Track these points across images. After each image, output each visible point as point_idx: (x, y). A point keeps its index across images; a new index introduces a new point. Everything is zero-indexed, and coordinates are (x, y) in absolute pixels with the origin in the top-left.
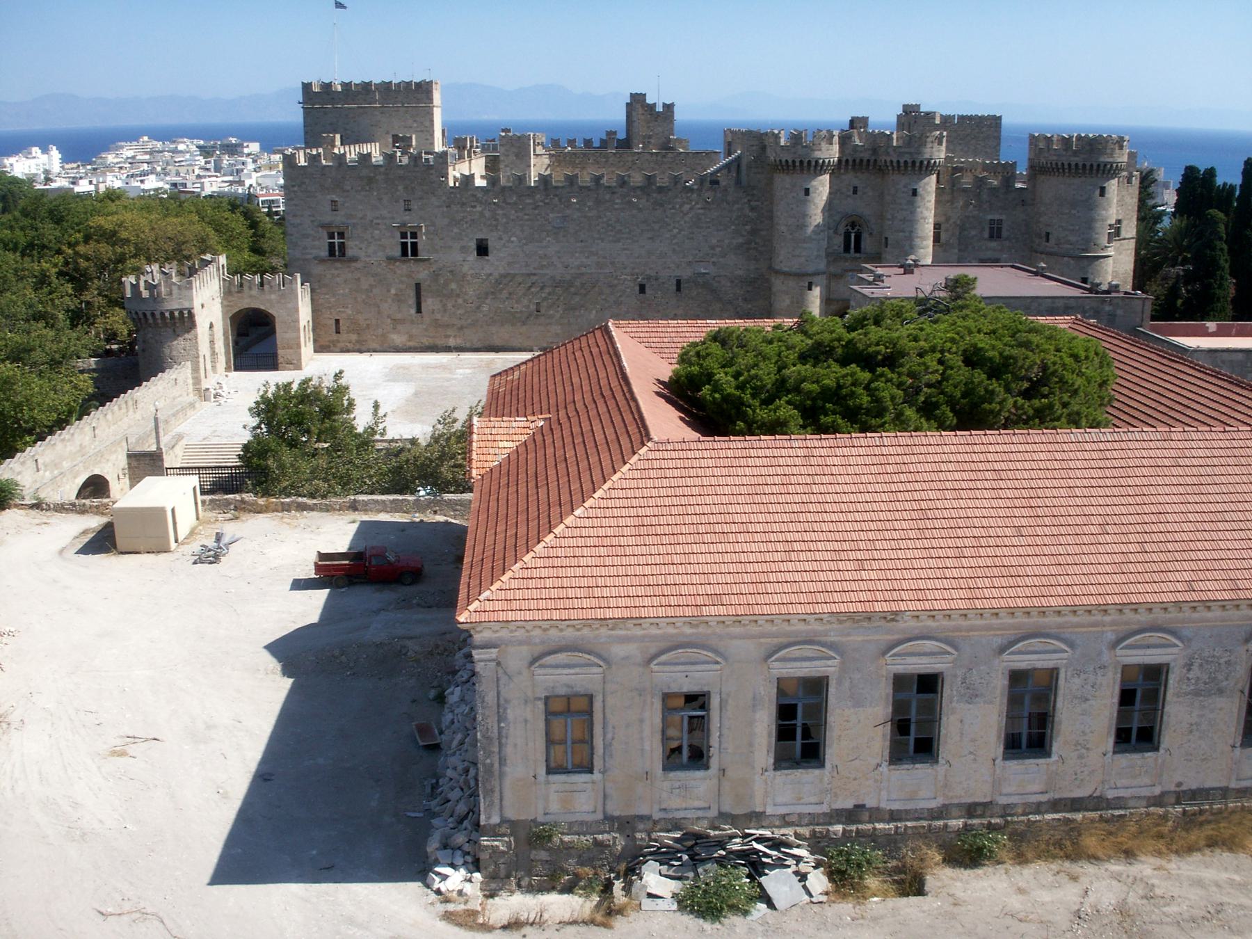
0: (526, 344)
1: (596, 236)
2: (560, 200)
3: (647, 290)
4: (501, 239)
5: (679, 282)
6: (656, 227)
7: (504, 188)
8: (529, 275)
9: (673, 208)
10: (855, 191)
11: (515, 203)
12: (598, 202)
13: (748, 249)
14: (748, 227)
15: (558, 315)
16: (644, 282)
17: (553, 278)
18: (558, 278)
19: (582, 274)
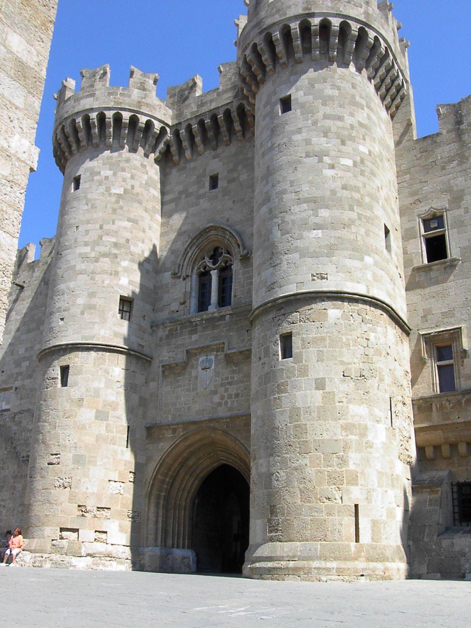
10: (214, 182)
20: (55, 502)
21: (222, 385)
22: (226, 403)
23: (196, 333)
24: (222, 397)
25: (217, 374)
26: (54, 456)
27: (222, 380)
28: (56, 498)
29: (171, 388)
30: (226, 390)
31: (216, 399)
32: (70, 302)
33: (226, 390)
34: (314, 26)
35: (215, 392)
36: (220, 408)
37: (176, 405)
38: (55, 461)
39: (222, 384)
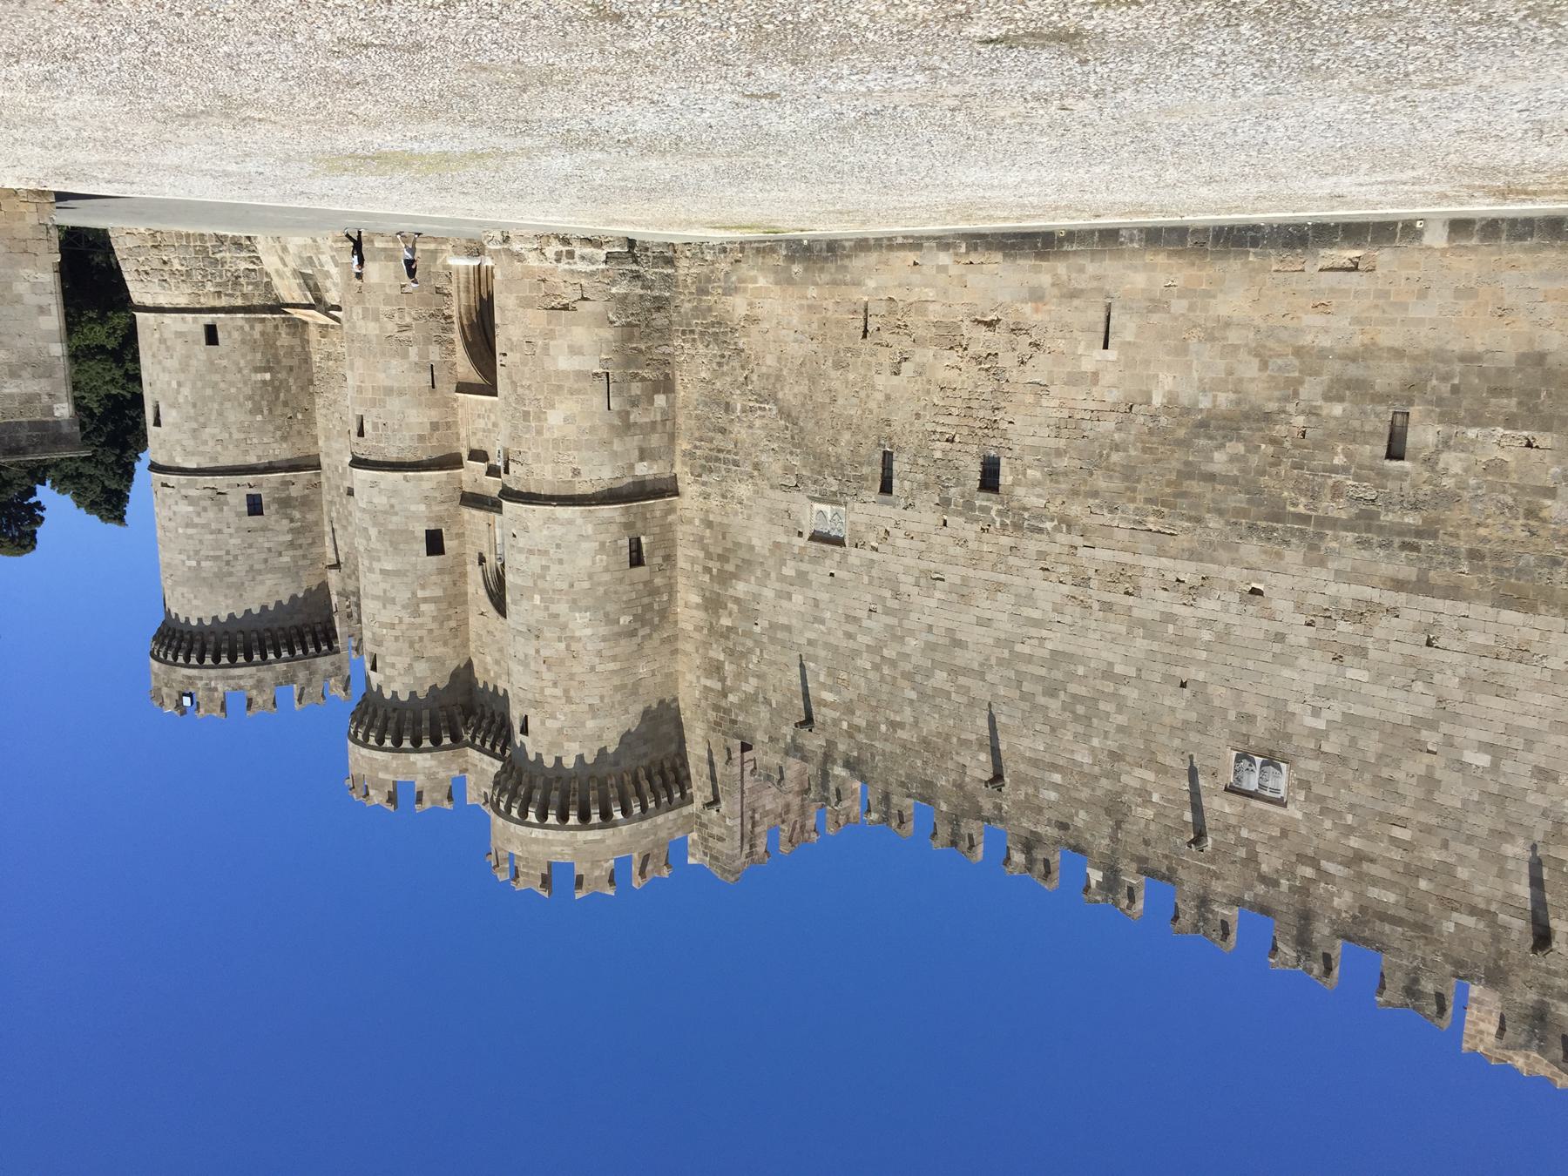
0: (1472, 262)
1: (1131, 694)
2: (1252, 859)
3: (974, 471)
4: (1545, 775)
5: (886, 488)
6: (940, 677)
7: (1496, 978)
8: (1422, 587)
9: (894, 725)
11: (1449, 905)
12: (1115, 810)
13: (723, 558)
14: (726, 622)
15: (1311, 390)
16: (982, 500)
17: (1316, 556)
18: (1293, 556)
19: (1193, 555)
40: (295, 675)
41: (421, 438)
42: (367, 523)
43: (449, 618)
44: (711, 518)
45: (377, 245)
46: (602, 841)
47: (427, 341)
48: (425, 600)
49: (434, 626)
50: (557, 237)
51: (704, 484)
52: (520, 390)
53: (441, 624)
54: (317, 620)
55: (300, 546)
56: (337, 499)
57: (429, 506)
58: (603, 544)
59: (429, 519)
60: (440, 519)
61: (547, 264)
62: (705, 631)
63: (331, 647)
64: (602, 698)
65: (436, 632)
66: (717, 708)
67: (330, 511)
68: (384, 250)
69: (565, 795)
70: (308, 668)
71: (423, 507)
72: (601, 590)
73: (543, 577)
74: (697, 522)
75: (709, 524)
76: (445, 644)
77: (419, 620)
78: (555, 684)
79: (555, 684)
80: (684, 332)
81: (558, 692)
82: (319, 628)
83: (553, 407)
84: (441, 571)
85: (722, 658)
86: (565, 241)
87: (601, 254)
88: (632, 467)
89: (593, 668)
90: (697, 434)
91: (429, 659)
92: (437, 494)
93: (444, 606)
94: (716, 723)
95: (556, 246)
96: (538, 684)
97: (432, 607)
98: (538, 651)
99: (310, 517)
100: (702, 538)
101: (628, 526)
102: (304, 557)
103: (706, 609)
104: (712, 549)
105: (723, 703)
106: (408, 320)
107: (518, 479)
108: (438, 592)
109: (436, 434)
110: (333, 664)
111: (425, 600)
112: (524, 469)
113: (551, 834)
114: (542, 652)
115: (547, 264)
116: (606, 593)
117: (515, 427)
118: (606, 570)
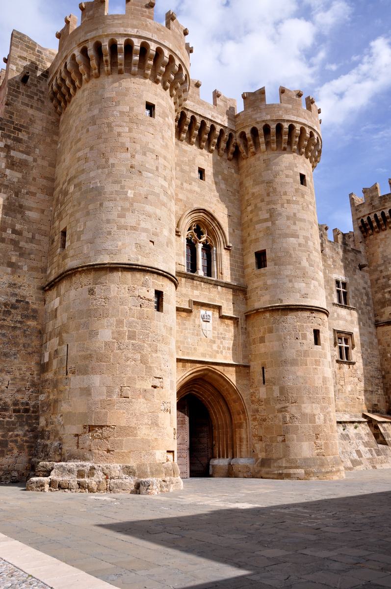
20: (162, 426)
21: (218, 338)
22: (222, 352)
23: (197, 290)
24: (219, 347)
25: (214, 328)
26: (157, 380)
27: (218, 334)
28: (163, 422)
29: (180, 328)
30: (222, 342)
31: (215, 347)
32: (158, 229)
33: (222, 342)
34: (120, 44)
35: (214, 342)
36: (218, 355)
37: (184, 344)
38: (158, 385)
39: (218, 336)
40: (380, 201)
41: (271, 331)
42: (310, 270)
43: (252, 212)
44: (9, 270)
45: (303, 471)
46: (86, 33)
47: (267, 401)
48: (266, 220)
49: (259, 205)
50: (91, 491)
51: (15, 295)
52: (138, 356)
53: (256, 206)
54: (372, 237)
55: (384, 277)
56: (363, 306)
57: (265, 284)
58: (79, 239)
59: (264, 275)
60: (258, 276)
61: (103, 465)
62: (24, 191)
63: (362, 221)
64: (88, 131)
65: (259, 200)
66: (18, 140)
67: (368, 299)
68: (297, 467)
69: (114, 63)
70: (373, 206)
71: (269, 282)
72: (83, 204)
73: (123, 209)
74: (25, 268)
75: (11, 264)
76: (253, 194)
77: (269, 207)
78: (119, 134)
79: (119, 134)
80: (26, 411)
81: (117, 129)
82: (370, 232)
83: (106, 344)
84: (257, 240)
85: (8, 172)
86: (81, 486)
87: (53, 476)
88: (60, 303)
89: (92, 148)
90: (18, 332)
91: (263, 182)
92: (260, 292)
93: (255, 219)
94: (20, 130)
95: (92, 482)
96: (134, 134)
97: (261, 217)
98: (133, 156)
99: (379, 295)
100: (21, 255)
101: (65, 257)
102: (381, 271)
103: (21, 206)
104: (12, 247)
105: (9, 142)
106: (280, 415)
107: (144, 284)
108: (258, 227)
109: (261, 335)
110: (360, 211)
111: (266, 220)
112: (137, 293)
113: (121, 30)
114: (129, 155)
115: (103, 465)
116: (80, 204)
117: (144, 327)
118: (78, 221)
